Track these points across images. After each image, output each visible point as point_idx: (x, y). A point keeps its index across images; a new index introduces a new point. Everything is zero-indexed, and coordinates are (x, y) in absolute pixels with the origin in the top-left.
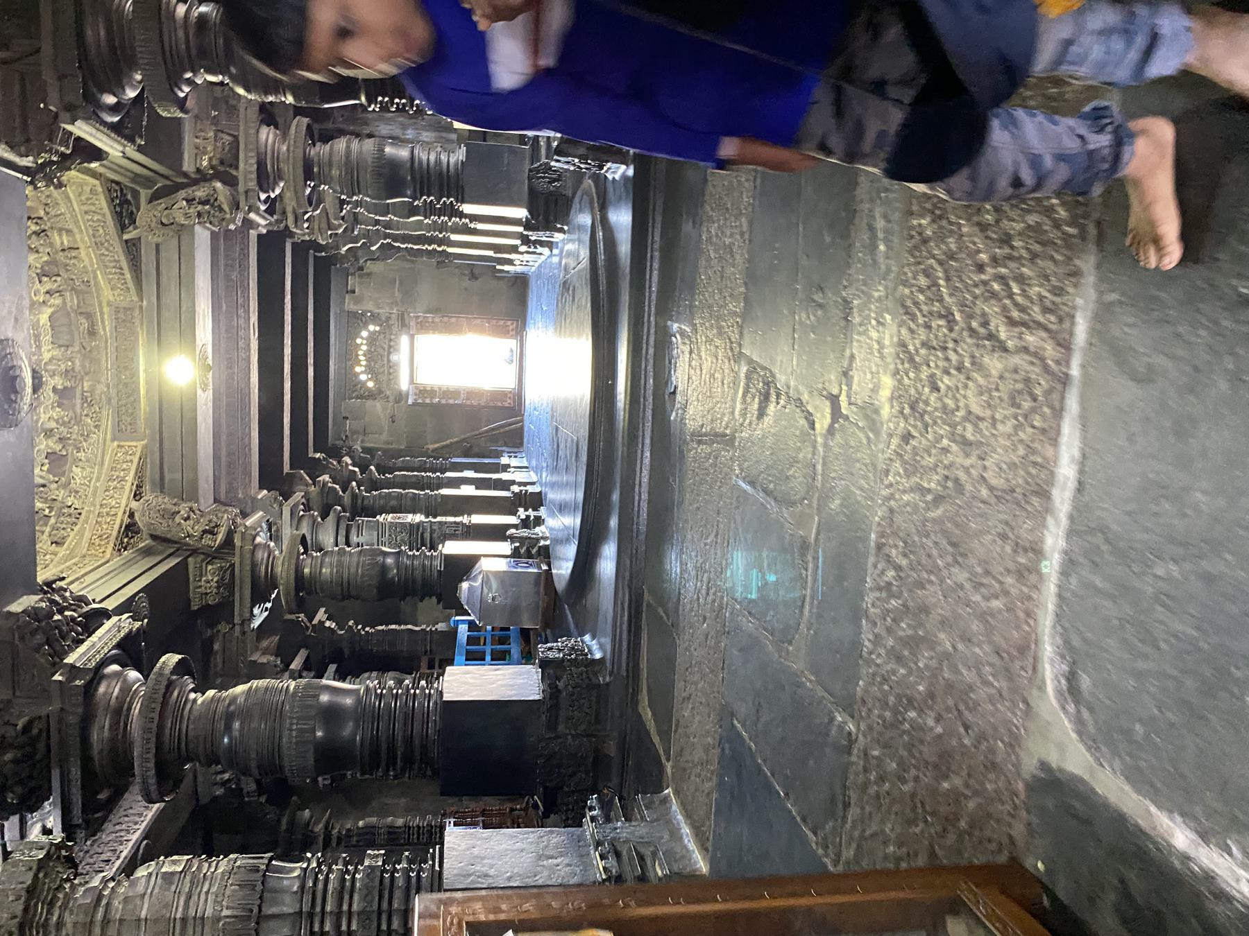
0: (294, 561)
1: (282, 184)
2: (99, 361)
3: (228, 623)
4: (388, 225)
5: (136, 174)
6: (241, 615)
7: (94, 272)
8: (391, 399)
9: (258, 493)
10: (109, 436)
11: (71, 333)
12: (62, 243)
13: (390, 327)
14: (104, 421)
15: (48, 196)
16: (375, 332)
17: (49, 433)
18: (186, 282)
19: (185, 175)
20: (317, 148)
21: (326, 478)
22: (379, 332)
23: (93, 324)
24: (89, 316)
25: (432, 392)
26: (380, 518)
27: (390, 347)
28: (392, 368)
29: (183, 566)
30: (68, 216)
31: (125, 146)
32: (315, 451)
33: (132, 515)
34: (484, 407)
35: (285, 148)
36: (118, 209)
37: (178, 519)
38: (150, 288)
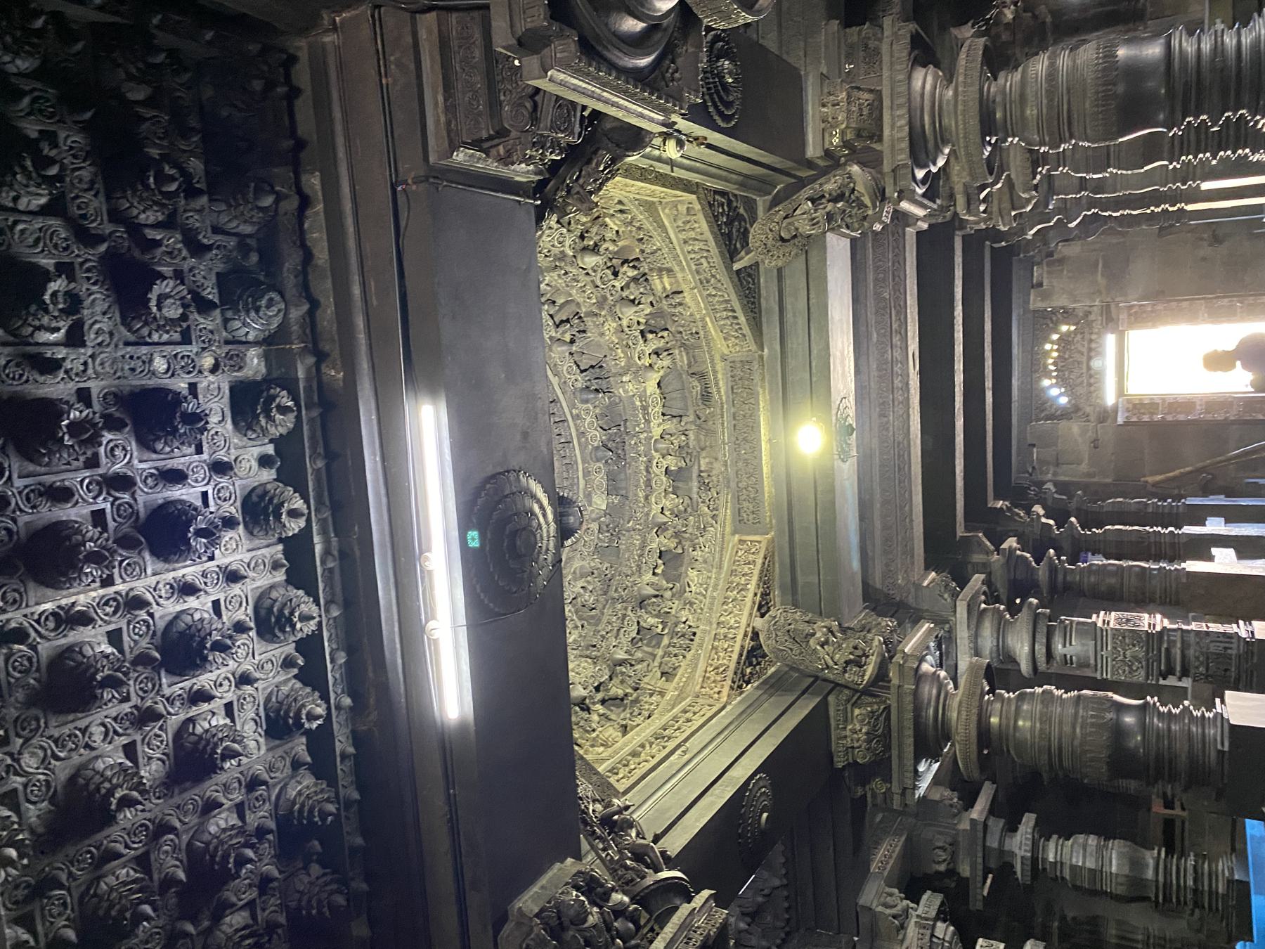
0: (975, 703)
1: (947, 151)
2: (714, 432)
3: (885, 781)
4: (1099, 186)
5: (745, 176)
6: (901, 781)
7: (703, 320)
8: (1092, 418)
9: (924, 577)
10: (728, 529)
11: (684, 398)
12: (664, 288)
13: (1089, 324)
14: (722, 510)
15: (639, 229)
16: (1069, 333)
17: (661, 528)
18: (816, 315)
19: (810, 164)
20: (1001, 80)
21: (1012, 542)
23: (706, 388)
24: (701, 376)
25: (1148, 405)
26: (1099, 619)
27: (1090, 350)
28: (1093, 380)
29: (820, 713)
30: (665, 250)
31: (666, 111)
32: (997, 498)
33: (755, 635)
34: (1233, 422)
35: (951, 93)
36: (725, 230)
37: (812, 642)
38: (771, 330)
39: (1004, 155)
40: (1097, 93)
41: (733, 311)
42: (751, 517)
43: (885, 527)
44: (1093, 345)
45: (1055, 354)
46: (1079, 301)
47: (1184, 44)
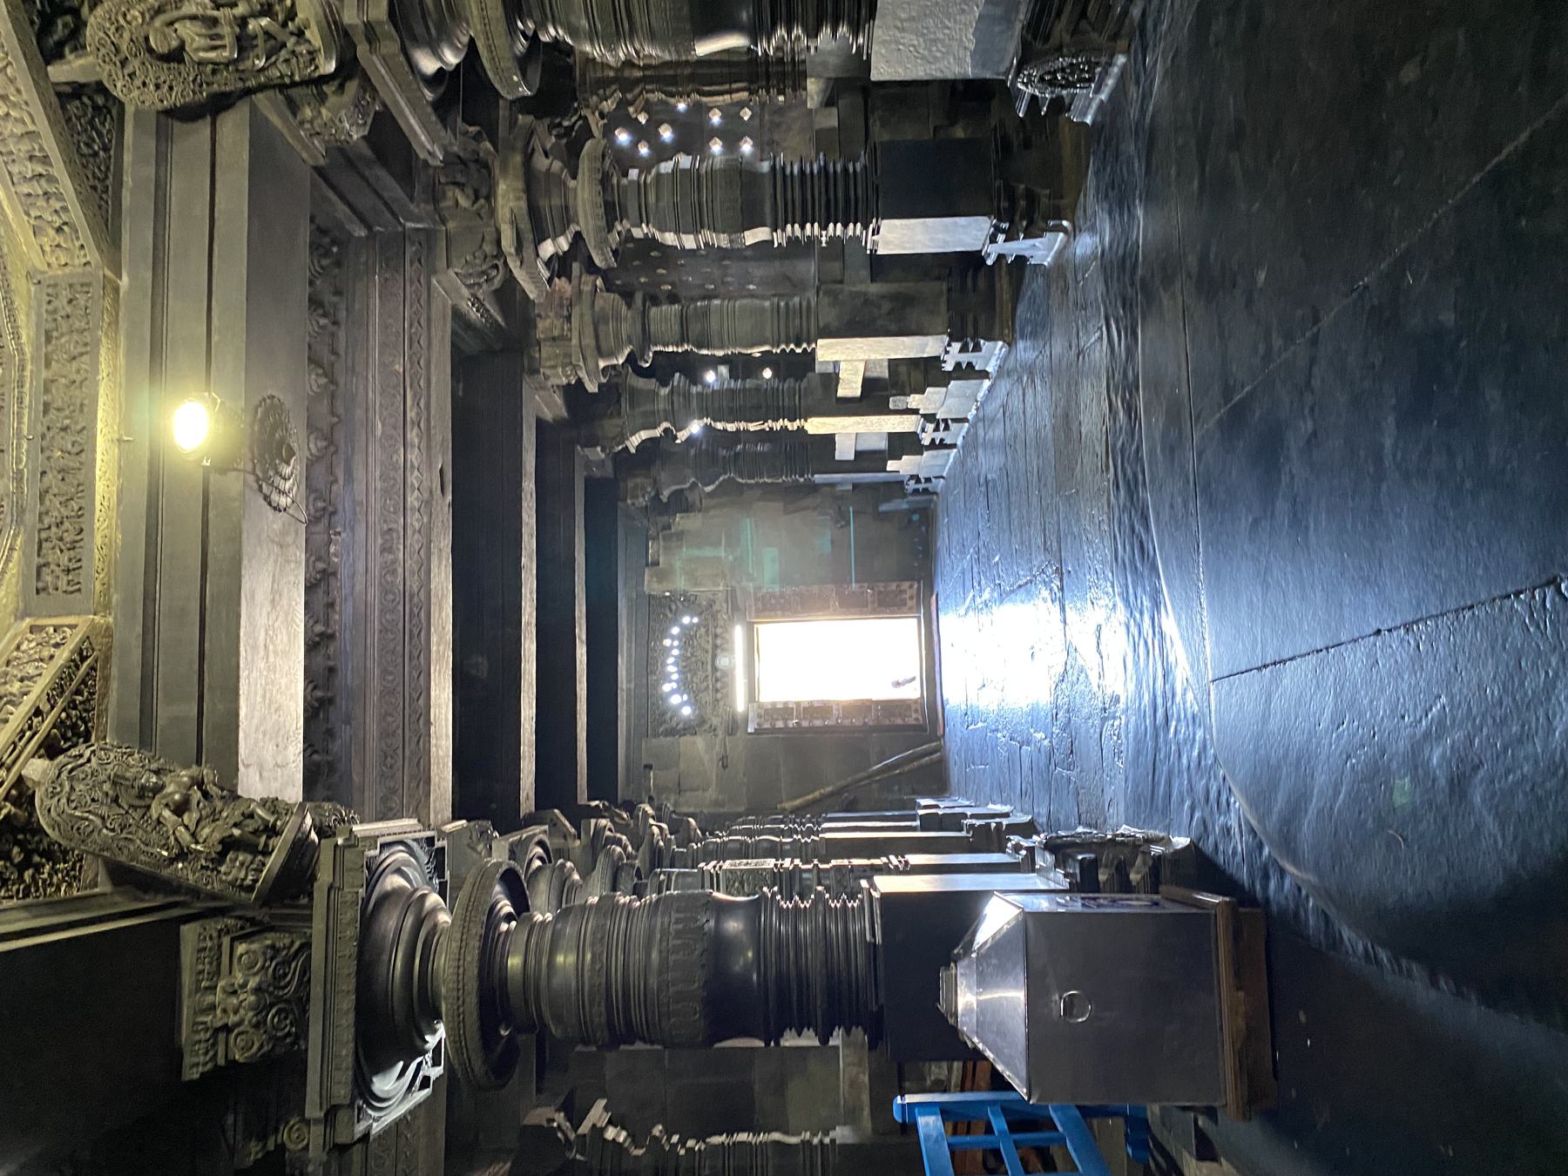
13: (714, 617)
22: (698, 626)
25: (786, 711)
32: (590, 799)
34: (873, 729)
38: (136, 235)
39: (571, 196)
41: (45, 160)
42: (64, 579)
43: (385, 734)
44: (719, 642)
45: (676, 652)
46: (700, 585)
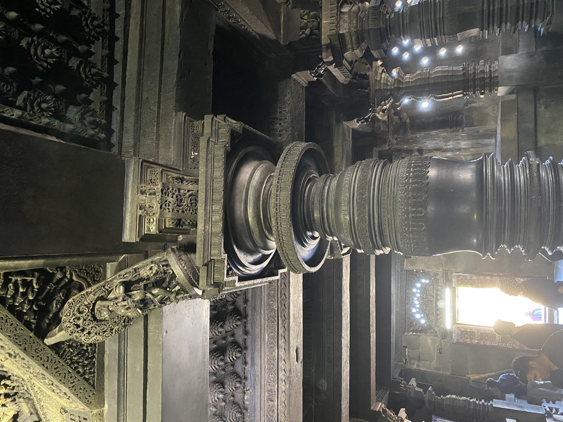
13: (437, 281)
27: (437, 295)
40: (407, 212)
45: (418, 295)
46: (430, 268)
47: (497, 173)
